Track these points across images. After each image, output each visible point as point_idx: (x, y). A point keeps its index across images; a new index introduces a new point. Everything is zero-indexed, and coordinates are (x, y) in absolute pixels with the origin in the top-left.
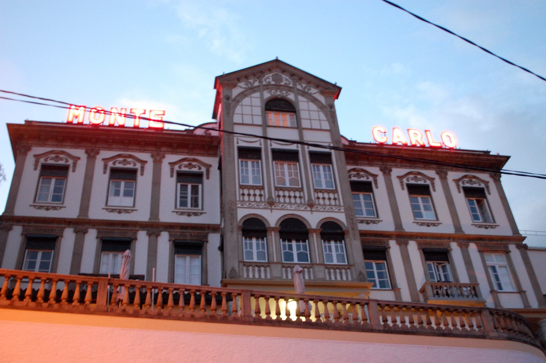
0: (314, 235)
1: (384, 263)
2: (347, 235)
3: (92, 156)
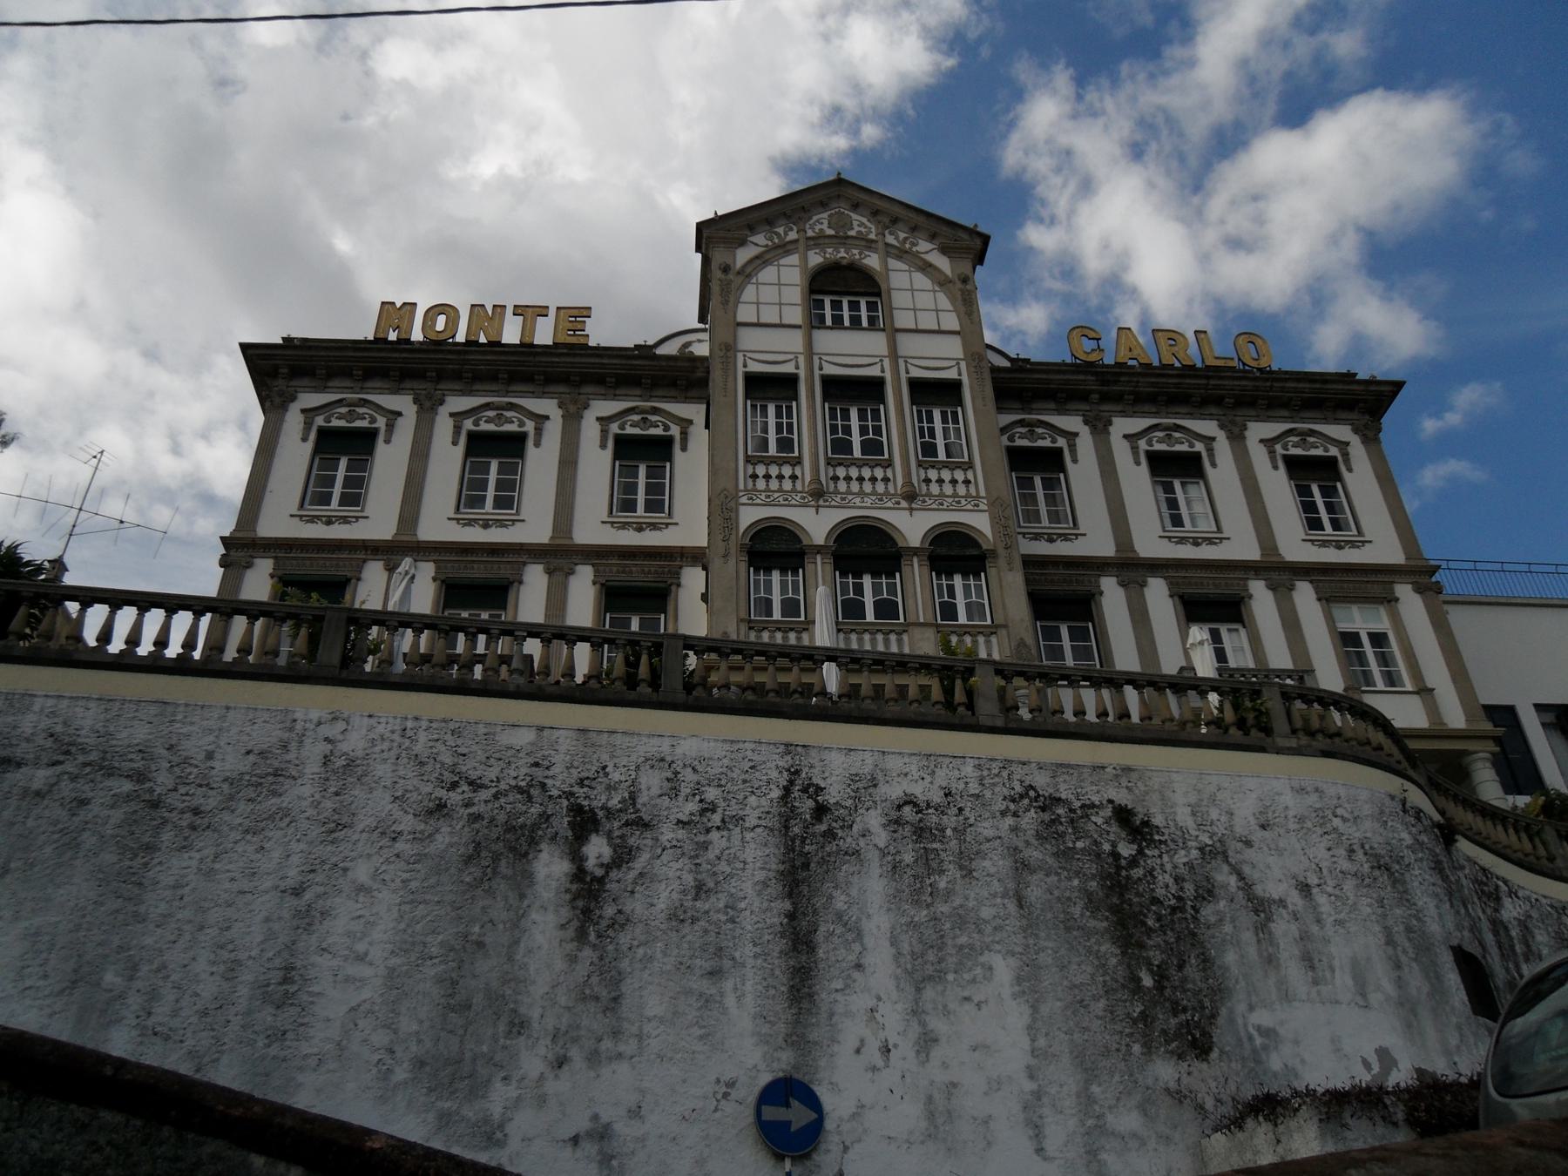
0: (915, 560)
3: (427, 408)
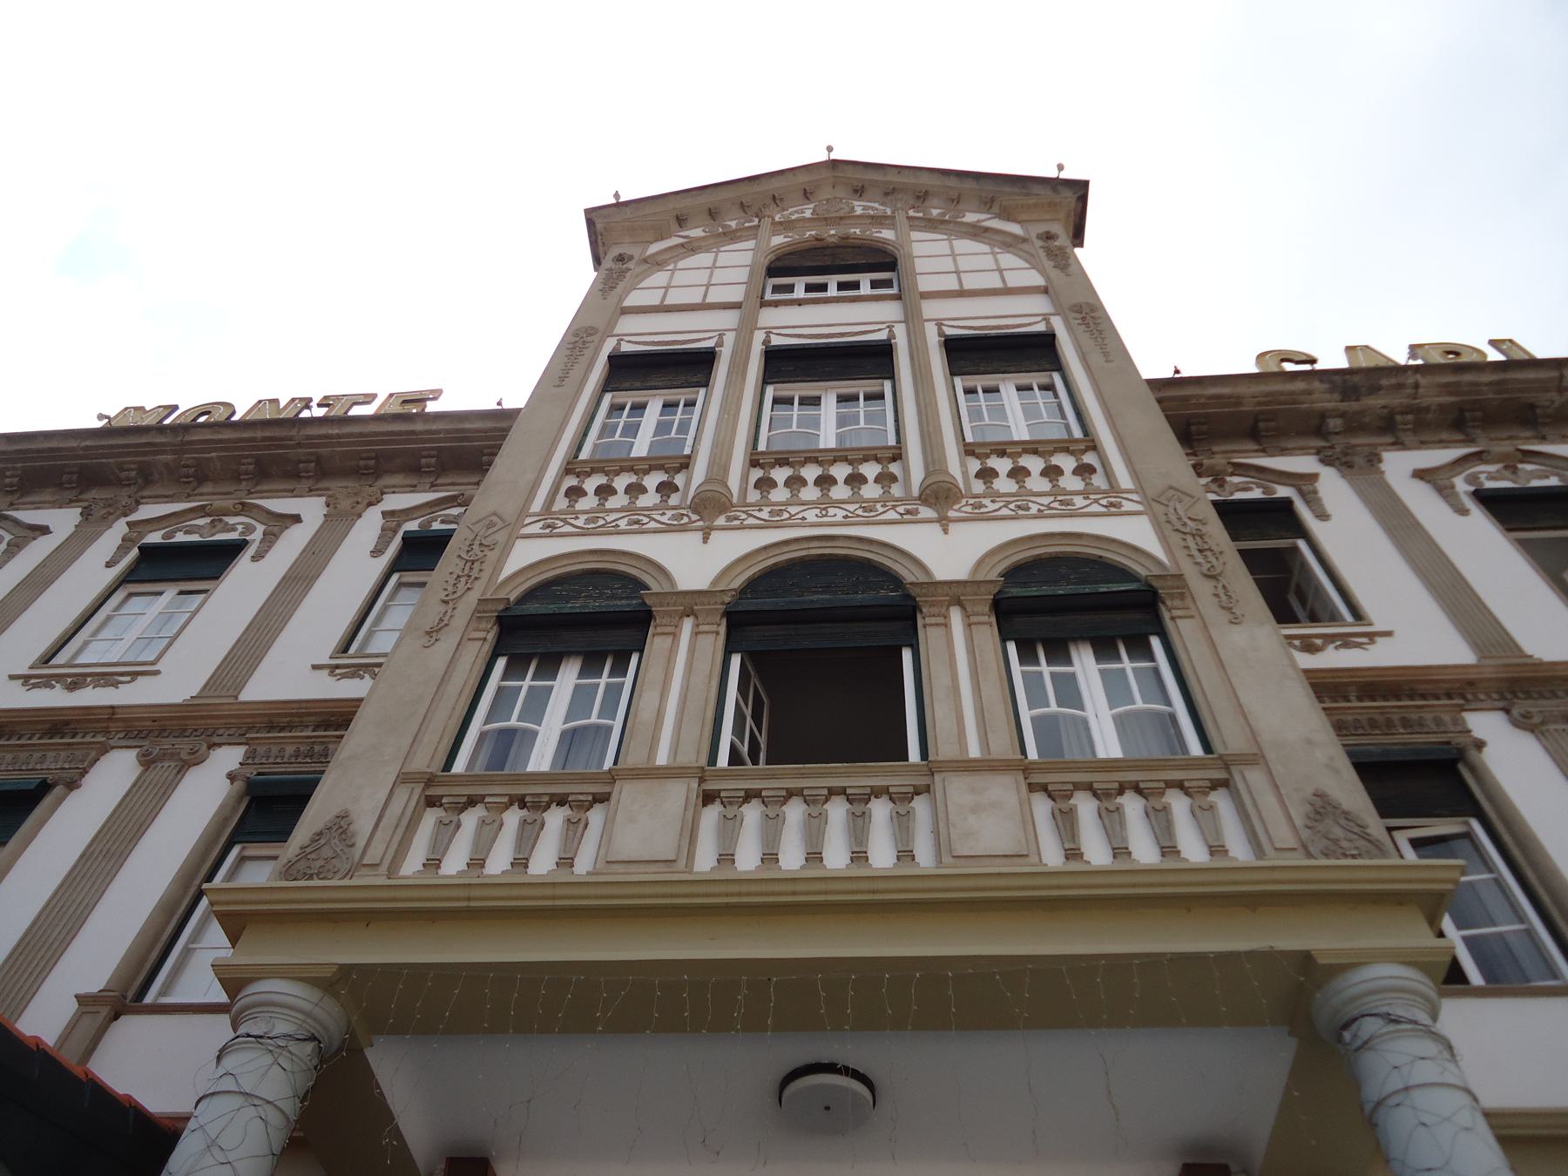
0: (956, 616)
1: (1468, 836)
2: (1177, 603)
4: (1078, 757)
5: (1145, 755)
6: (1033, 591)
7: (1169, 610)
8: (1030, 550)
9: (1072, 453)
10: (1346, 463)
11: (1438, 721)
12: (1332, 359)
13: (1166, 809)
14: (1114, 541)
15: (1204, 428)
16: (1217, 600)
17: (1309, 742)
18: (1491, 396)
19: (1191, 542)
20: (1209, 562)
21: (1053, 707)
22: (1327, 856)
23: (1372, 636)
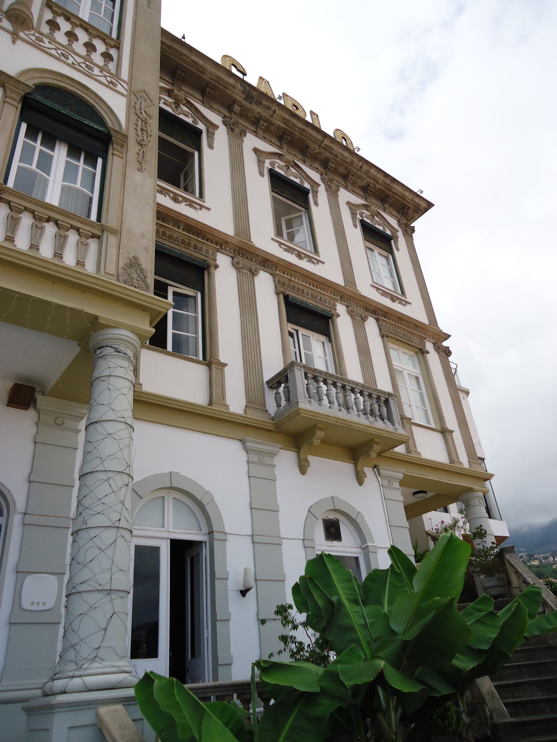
1: (195, 298)
2: (118, 148)
4: (39, 198)
5: (72, 211)
6: (49, 103)
7: (113, 150)
8: (58, 81)
9: (106, 44)
10: (231, 128)
11: (207, 251)
12: (252, 79)
13: (65, 237)
14: (103, 101)
15: (183, 75)
16: (137, 156)
17: (143, 235)
18: (297, 134)
19: (140, 123)
20: (143, 137)
21: (34, 167)
22: (125, 283)
23: (202, 207)
